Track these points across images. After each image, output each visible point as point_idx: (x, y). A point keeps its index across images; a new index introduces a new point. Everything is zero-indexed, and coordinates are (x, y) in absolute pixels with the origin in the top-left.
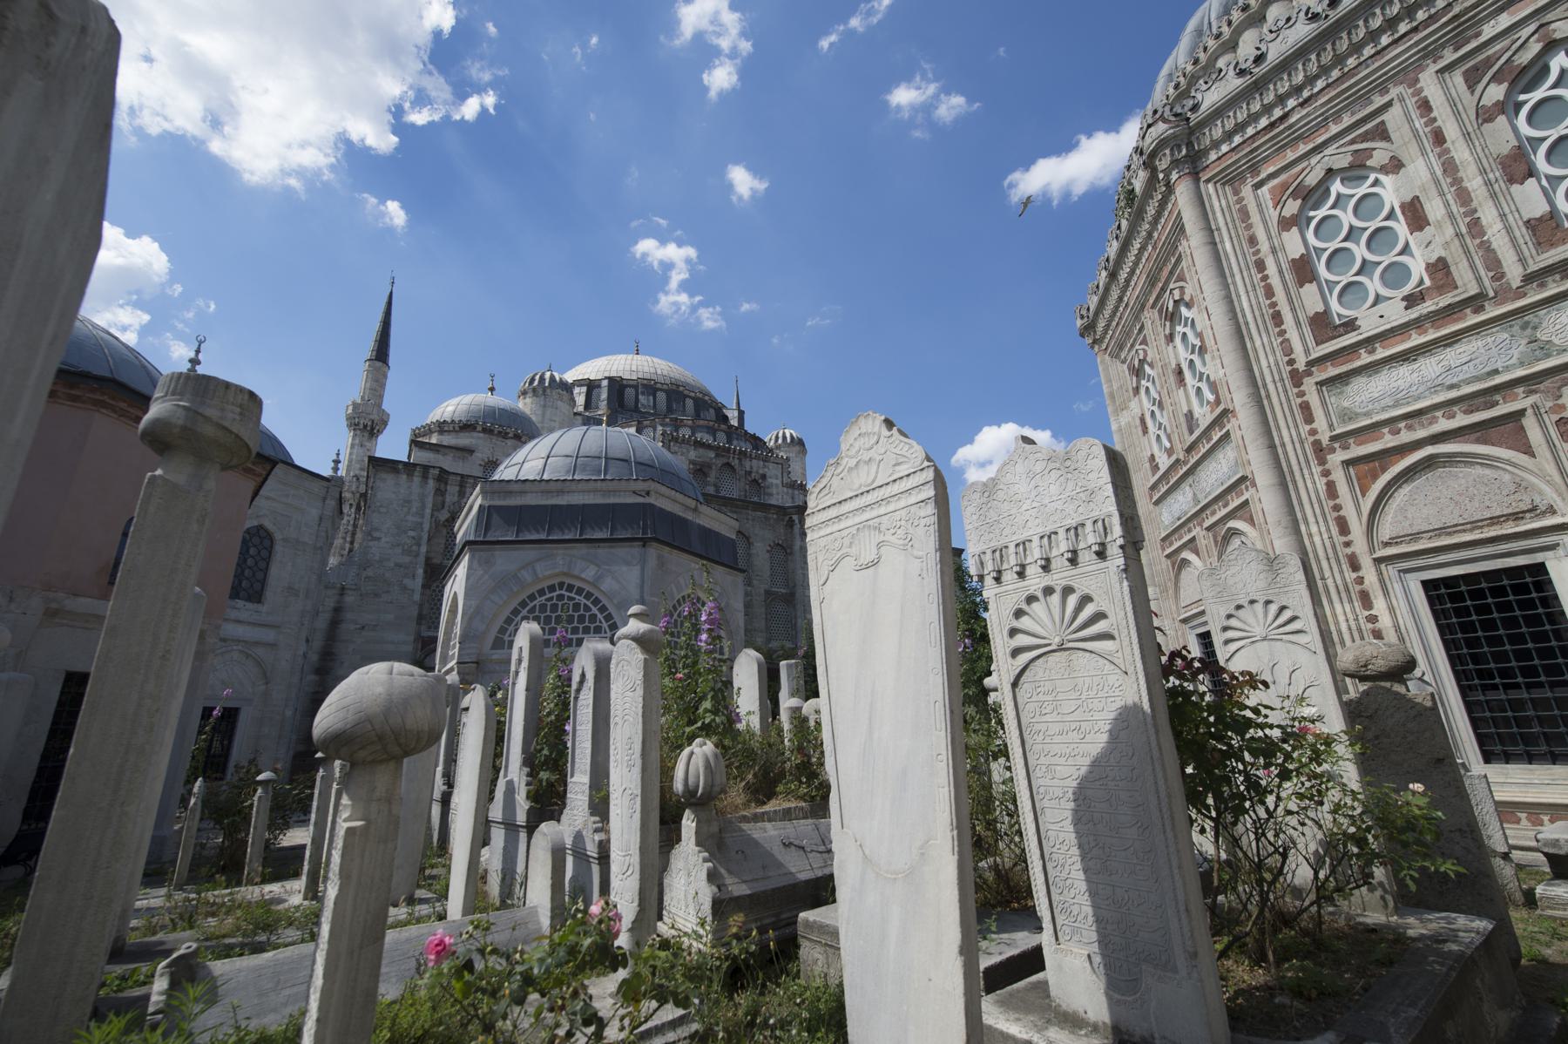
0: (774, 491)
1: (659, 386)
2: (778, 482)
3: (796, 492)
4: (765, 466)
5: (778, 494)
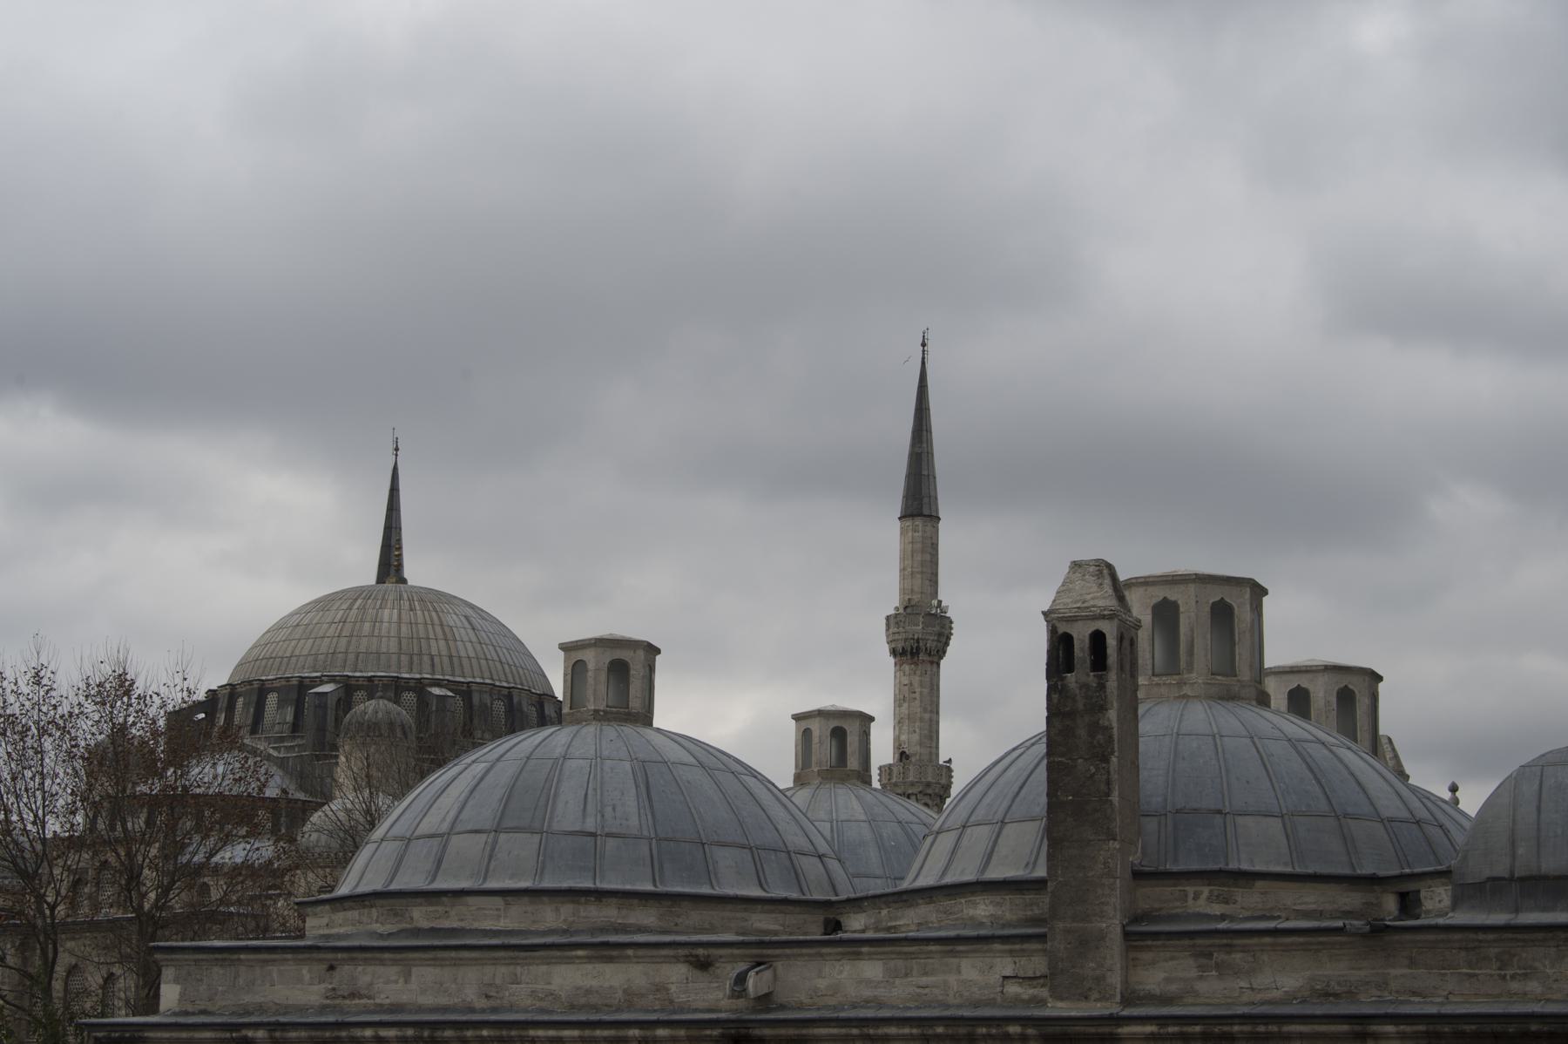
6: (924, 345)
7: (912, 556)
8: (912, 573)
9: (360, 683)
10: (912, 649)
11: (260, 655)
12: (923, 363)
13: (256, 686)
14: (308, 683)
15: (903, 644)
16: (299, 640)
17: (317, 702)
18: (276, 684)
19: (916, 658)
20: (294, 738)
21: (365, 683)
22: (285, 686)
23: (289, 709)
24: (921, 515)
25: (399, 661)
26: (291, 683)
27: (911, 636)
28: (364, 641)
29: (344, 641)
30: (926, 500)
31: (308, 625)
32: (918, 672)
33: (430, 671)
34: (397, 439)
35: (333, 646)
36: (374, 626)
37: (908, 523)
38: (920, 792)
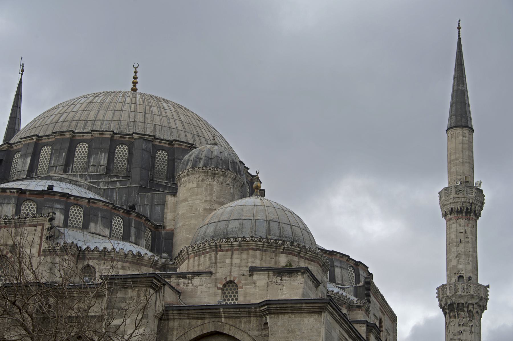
1: (45, 140)
2: (35, 251)
4: (17, 234)
6: (459, 28)
7: (463, 152)
8: (463, 162)
9: (162, 144)
10: (467, 209)
11: (59, 119)
12: (459, 38)
13: (68, 136)
14: (118, 139)
15: (461, 205)
16: (99, 110)
17: (144, 147)
18: (88, 137)
19: (468, 216)
20: (111, 176)
21: (167, 146)
22: (98, 138)
23: (103, 155)
24: (467, 127)
26: (104, 136)
27: (468, 201)
30: (469, 119)
32: (470, 225)
34: (23, 64)
36: (161, 110)
37: (458, 131)
38: (476, 303)
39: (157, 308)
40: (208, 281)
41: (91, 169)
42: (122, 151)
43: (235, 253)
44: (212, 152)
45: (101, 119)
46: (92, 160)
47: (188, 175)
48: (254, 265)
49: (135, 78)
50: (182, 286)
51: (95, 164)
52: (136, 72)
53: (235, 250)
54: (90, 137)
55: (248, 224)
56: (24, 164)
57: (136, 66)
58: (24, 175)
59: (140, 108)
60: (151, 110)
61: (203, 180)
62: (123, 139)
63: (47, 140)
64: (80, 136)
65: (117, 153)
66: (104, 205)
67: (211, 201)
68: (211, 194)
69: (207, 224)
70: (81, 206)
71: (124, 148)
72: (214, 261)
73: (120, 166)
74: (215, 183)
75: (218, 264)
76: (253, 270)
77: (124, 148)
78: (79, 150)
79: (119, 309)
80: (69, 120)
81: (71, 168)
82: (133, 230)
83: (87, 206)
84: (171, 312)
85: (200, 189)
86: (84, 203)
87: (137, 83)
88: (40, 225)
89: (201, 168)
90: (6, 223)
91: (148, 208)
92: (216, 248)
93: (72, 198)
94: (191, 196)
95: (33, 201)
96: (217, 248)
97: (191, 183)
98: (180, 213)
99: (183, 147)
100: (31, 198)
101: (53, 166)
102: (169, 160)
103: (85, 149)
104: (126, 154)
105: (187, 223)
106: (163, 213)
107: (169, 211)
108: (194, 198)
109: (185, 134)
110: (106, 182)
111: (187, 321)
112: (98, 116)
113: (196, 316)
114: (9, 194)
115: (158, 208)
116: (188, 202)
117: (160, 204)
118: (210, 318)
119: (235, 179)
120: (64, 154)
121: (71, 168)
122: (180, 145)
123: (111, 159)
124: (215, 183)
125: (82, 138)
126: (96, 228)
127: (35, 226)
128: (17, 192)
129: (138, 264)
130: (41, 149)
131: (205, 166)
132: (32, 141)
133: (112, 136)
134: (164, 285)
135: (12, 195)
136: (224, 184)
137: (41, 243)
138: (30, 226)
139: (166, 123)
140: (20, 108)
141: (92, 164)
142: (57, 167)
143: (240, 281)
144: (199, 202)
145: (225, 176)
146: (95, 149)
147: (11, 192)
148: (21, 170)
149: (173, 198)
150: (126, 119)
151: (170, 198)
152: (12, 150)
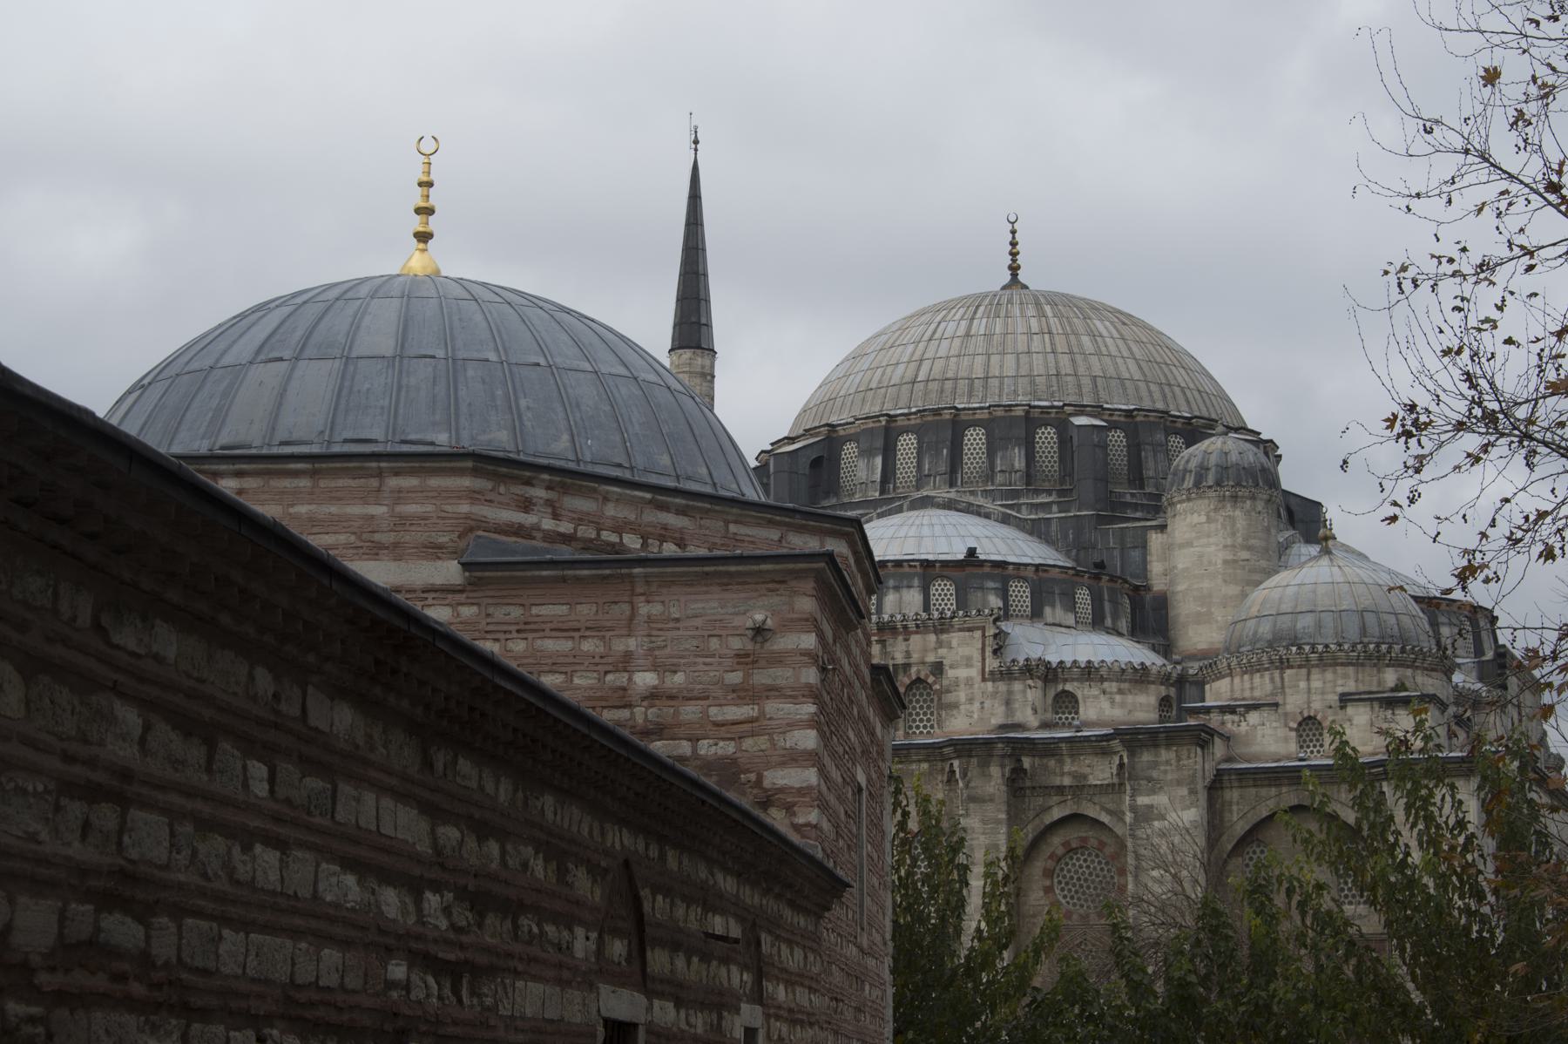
0: (962, 695)
1: (901, 422)
2: (974, 672)
3: (1017, 686)
4: (940, 644)
5: (971, 700)
11: (916, 376)
13: (948, 417)
16: (989, 355)
18: (984, 415)
20: (1037, 492)
21: (1122, 419)
23: (1016, 450)
25: (1150, 392)
26: (1013, 414)
28: (1094, 360)
29: (1065, 361)
31: (988, 336)
33: (1187, 409)
34: (696, 128)
35: (1052, 364)
36: (1096, 341)
39: (1207, 773)
40: (1273, 718)
41: (999, 478)
42: (1046, 438)
43: (1314, 671)
44: (1226, 454)
45: (997, 374)
46: (999, 462)
47: (1189, 500)
48: (1346, 690)
49: (1014, 244)
50: (1229, 725)
51: (1004, 468)
52: (1013, 232)
53: (1313, 666)
54: (987, 416)
55: (1328, 619)
56: (870, 469)
57: (1012, 220)
58: (876, 491)
59: (1061, 346)
60: (1080, 345)
61: (1216, 510)
62: (1045, 416)
63: (906, 423)
64: (966, 414)
65: (1038, 443)
66: (1062, 573)
67: (1233, 546)
68: (1233, 534)
69: (1257, 617)
70: (1025, 579)
71: (1049, 433)
72: (1279, 684)
73: (1047, 466)
74: (1238, 513)
75: (1287, 690)
76: (1345, 700)
77: (1049, 433)
78: (969, 440)
79: (1150, 779)
80: (937, 377)
81: (959, 475)
82: (1107, 606)
83: (1035, 577)
84: (1226, 778)
85: (1213, 526)
86: (1030, 573)
87: (1018, 253)
88: (977, 628)
89: (1210, 487)
90: (917, 626)
91: (1116, 553)
92: (1282, 663)
93: (1011, 567)
94: (1198, 538)
95: (949, 578)
96: (1283, 664)
97: (1196, 515)
98: (1180, 566)
99: (1152, 419)
100: (945, 573)
101: (929, 476)
102: (1128, 446)
103: (980, 439)
104: (1055, 443)
105: (1195, 586)
106: (1145, 562)
107: (1154, 558)
108: (1204, 541)
109: (1148, 387)
110: (1032, 504)
111: (1253, 791)
112: (991, 369)
113: (1266, 782)
114: (906, 569)
115: (1135, 554)
116: (1192, 549)
117: (1136, 547)
118: (1289, 785)
119: (1269, 501)
120: (945, 451)
121: (959, 475)
122: (1146, 416)
123: (1030, 457)
124: (1238, 513)
125: (971, 418)
126: (1054, 613)
127: (970, 630)
128: (921, 565)
129: (1142, 682)
130: (896, 440)
131: (1219, 483)
132: (878, 425)
133: (1027, 412)
134: (1212, 736)
135: (912, 570)
136: (1253, 514)
137: (984, 660)
138: (961, 630)
139: (1111, 372)
140: (702, 225)
141: (999, 469)
142: (935, 477)
143: (1325, 718)
144: (1213, 548)
145: (1253, 498)
146: (1001, 439)
147: (910, 566)
148: (867, 479)
149: (1160, 535)
150: (1042, 371)
151: (1154, 536)
152: (835, 435)
